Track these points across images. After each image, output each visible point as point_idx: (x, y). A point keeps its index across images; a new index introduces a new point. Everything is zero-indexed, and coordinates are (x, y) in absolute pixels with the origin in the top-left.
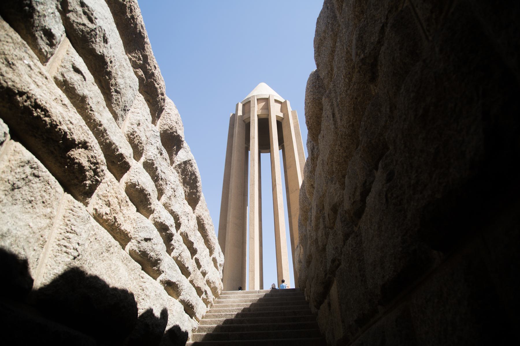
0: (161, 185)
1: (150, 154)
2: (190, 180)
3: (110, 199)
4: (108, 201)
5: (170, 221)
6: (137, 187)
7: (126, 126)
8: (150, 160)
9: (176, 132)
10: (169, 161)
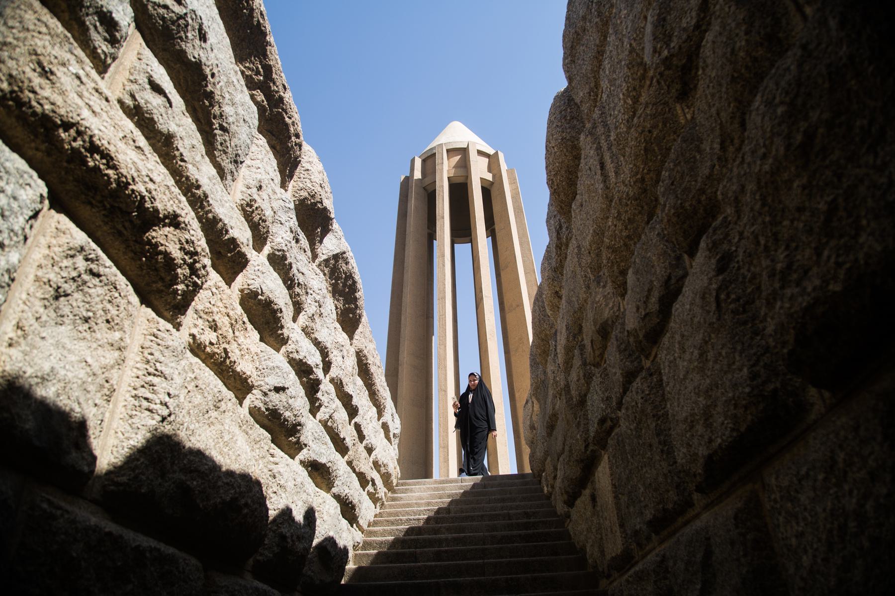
0: (298, 295)
1: (279, 240)
2: (344, 288)
3: (216, 318)
4: (214, 320)
5: (314, 359)
6: (260, 297)
7: (239, 191)
8: (279, 251)
9: (321, 203)
10: (309, 253)
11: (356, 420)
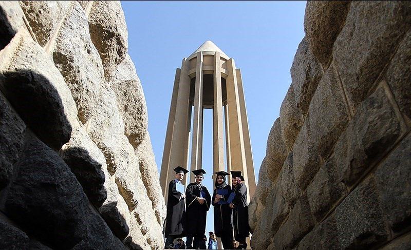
2: (131, 107)
6: (31, 85)
10: (101, 68)
11: (136, 210)
